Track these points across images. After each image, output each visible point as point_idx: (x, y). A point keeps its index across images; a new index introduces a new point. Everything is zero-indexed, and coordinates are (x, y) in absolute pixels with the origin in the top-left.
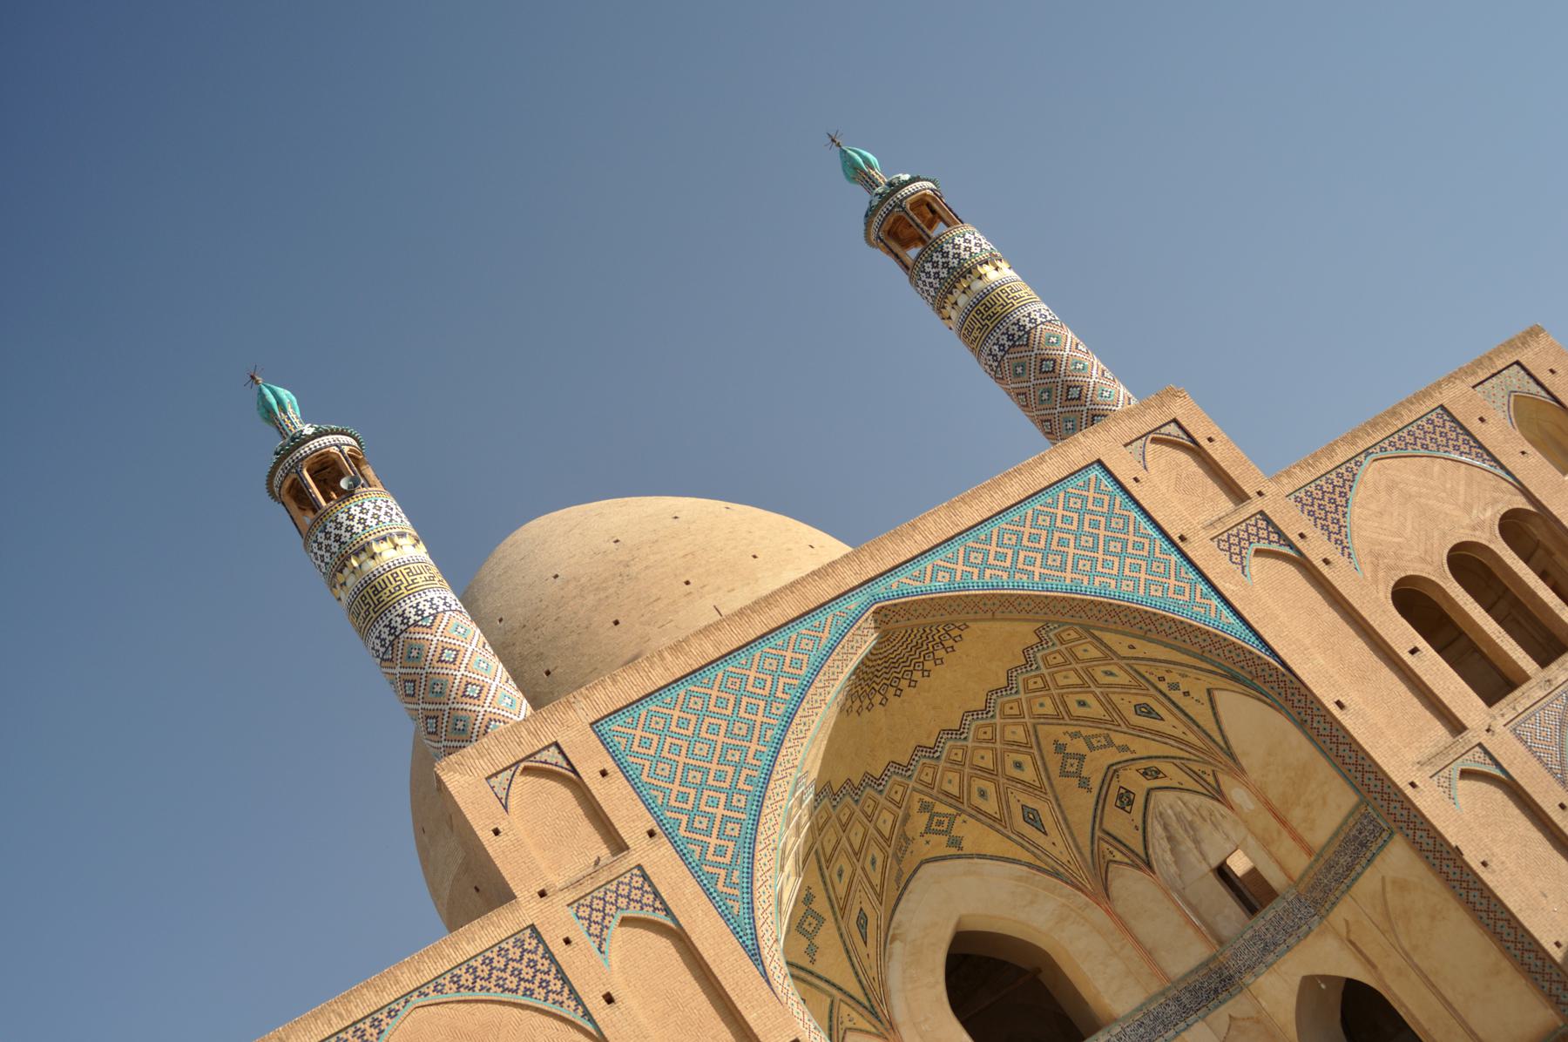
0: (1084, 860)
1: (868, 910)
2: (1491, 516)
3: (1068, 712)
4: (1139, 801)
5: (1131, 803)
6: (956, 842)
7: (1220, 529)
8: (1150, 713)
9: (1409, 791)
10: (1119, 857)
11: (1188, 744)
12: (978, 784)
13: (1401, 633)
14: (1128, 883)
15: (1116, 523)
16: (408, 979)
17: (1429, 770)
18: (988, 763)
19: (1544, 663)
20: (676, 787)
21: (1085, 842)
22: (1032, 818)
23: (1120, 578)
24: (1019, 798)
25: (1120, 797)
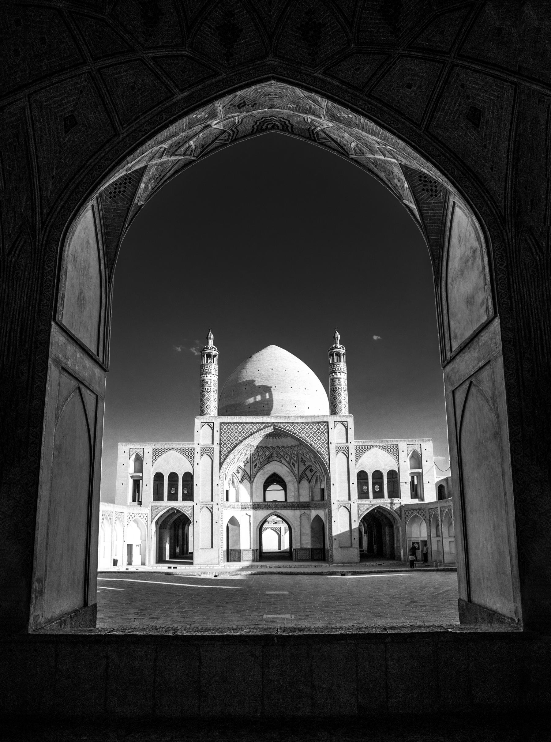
2: (389, 469)
4: (314, 472)
7: (339, 445)
9: (332, 504)
13: (354, 479)
14: (305, 483)
15: (322, 434)
16: (174, 446)
17: (338, 503)
18: (289, 453)
19: (374, 498)
20: (225, 438)
22: (294, 465)
23: (315, 444)
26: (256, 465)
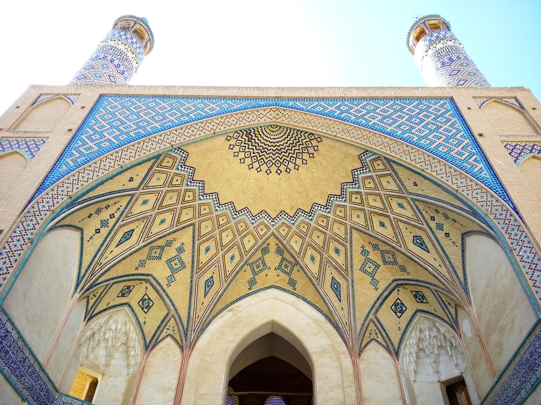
0: (355, 327)
1: (216, 279)
3: (372, 227)
5: (402, 312)
6: (292, 283)
8: (422, 245)
10: (380, 339)
11: (440, 273)
12: (310, 252)
21: (360, 317)
24: (330, 273)
25: (396, 304)
26: (209, 283)
